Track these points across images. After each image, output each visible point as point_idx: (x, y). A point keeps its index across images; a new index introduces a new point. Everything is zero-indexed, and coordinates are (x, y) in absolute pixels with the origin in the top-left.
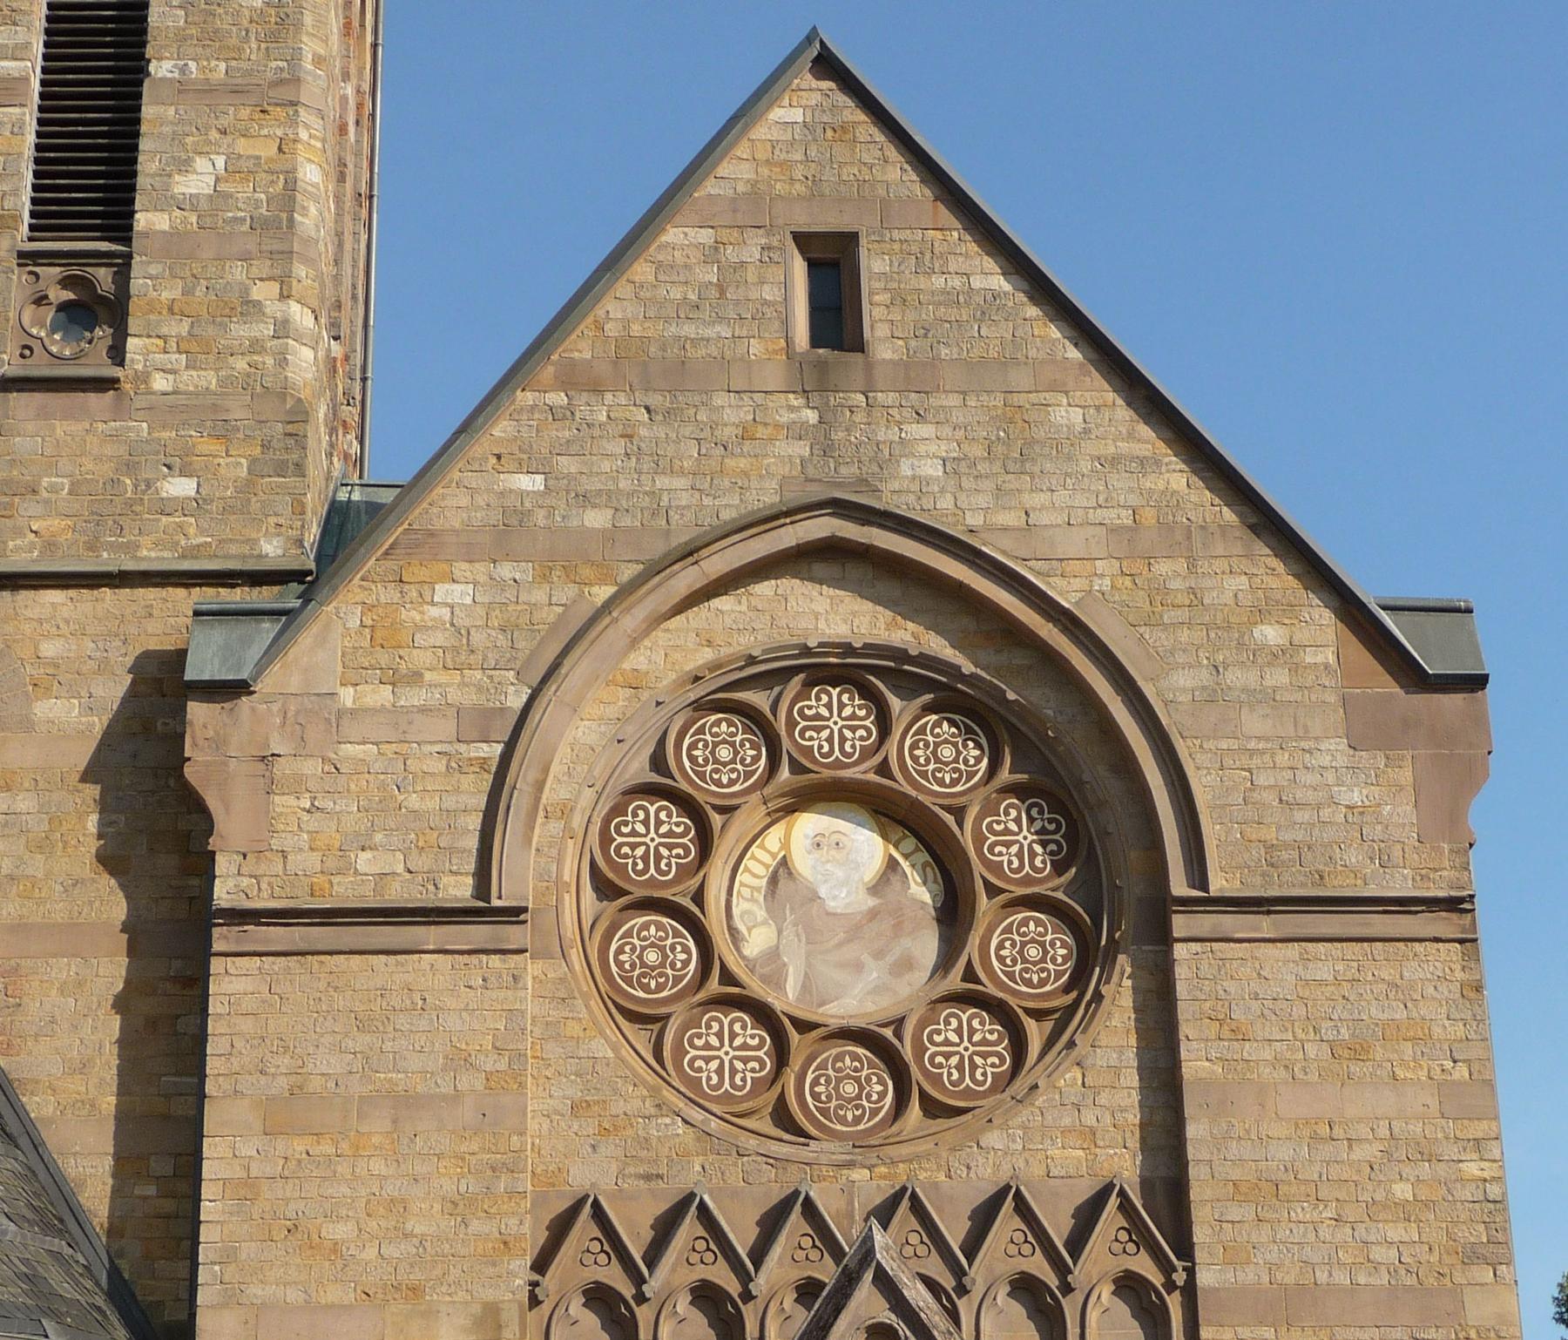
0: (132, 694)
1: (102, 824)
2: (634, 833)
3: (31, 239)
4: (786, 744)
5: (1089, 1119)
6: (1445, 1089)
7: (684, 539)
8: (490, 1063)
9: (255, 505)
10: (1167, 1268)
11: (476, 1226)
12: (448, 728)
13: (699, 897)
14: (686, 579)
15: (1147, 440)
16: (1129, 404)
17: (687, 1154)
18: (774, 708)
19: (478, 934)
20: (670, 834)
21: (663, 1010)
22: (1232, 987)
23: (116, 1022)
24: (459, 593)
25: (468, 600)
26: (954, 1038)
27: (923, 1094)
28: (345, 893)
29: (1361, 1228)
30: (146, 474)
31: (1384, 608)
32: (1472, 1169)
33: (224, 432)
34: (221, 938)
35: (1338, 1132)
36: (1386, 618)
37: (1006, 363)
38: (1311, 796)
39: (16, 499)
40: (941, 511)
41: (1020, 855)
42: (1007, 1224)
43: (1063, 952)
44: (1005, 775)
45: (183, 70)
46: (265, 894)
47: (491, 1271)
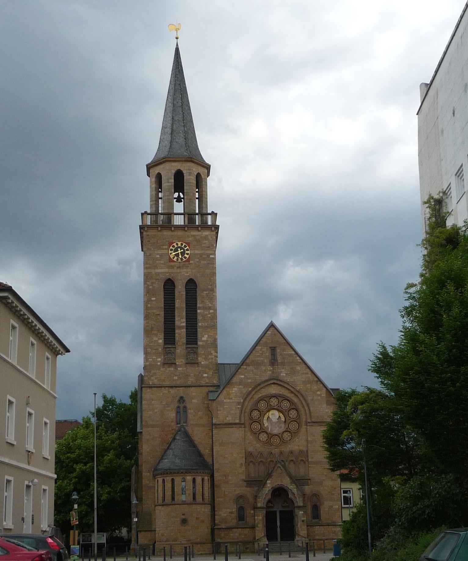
24: (236, 389)
45: (202, 324)
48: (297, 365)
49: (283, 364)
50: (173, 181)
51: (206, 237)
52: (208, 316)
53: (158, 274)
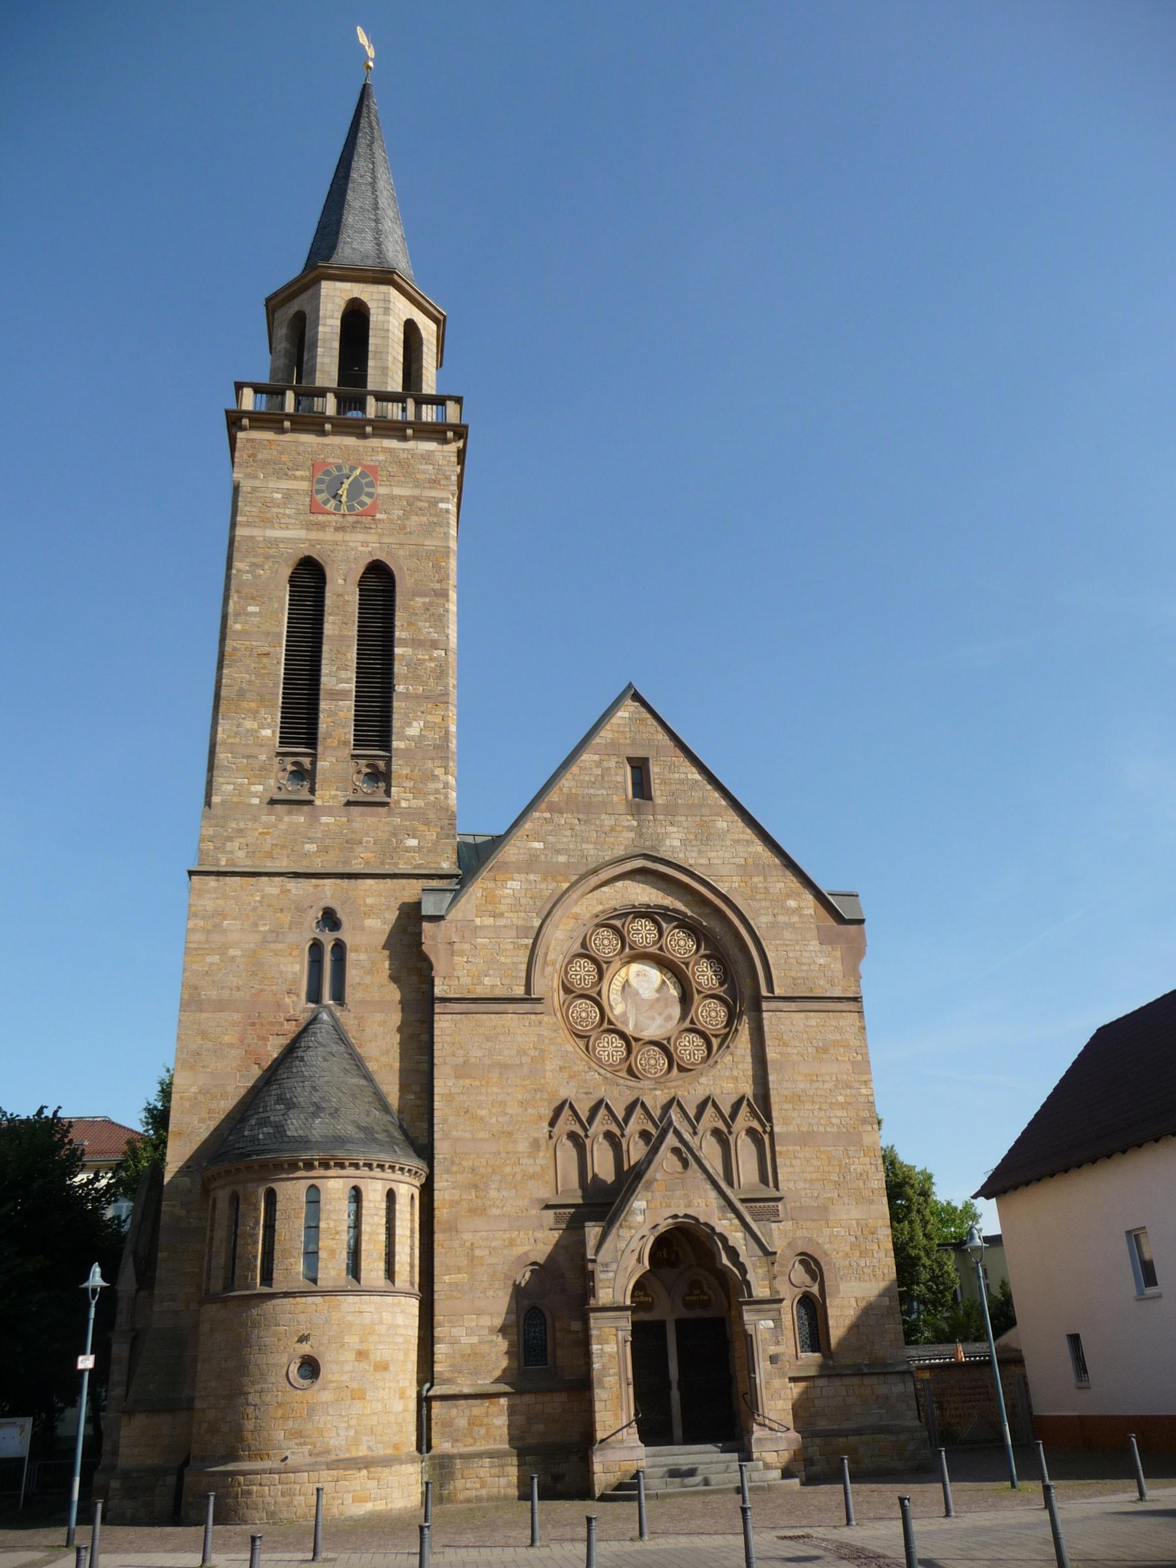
0: (399, 918)
1: (390, 964)
2: (576, 971)
3: (354, 749)
4: (627, 940)
5: (735, 1073)
6: (854, 1063)
7: (593, 867)
8: (532, 1053)
9: (439, 850)
10: (764, 1126)
11: (530, 1111)
12: (513, 933)
13: (599, 994)
14: (594, 881)
15: (748, 834)
16: (743, 821)
17: (599, 1085)
18: (623, 926)
19: (527, 1007)
20: (588, 971)
21: (588, 1034)
22: (782, 1027)
23: (398, 1036)
25: (519, 887)
26: (687, 1044)
27: (678, 1065)
28: (480, 992)
29: (828, 1112)
30: (400, 837)
31: (829, 894)
32: (864, 1091)
33: (427, 823)
34: (438, 1008)
35: (819, 1079)
36: (830, 898)
37: (701, 806)
38: (807, 961)
39: (355, 846)
40: (680, 858)
41: (708, 979)
42: (709, 1111)
43: (723, 1014)
44: (702, 952)
45: (407, 689)
46: (452, 992)
47: (534, 1127)
48: (717, 815)
49: (671, 810)
50: (338, 323)
51: (427, 457)
52: (428, 664)
53: (276, 542)
